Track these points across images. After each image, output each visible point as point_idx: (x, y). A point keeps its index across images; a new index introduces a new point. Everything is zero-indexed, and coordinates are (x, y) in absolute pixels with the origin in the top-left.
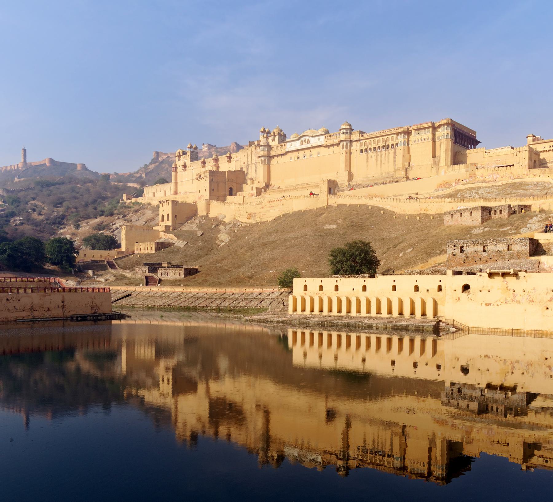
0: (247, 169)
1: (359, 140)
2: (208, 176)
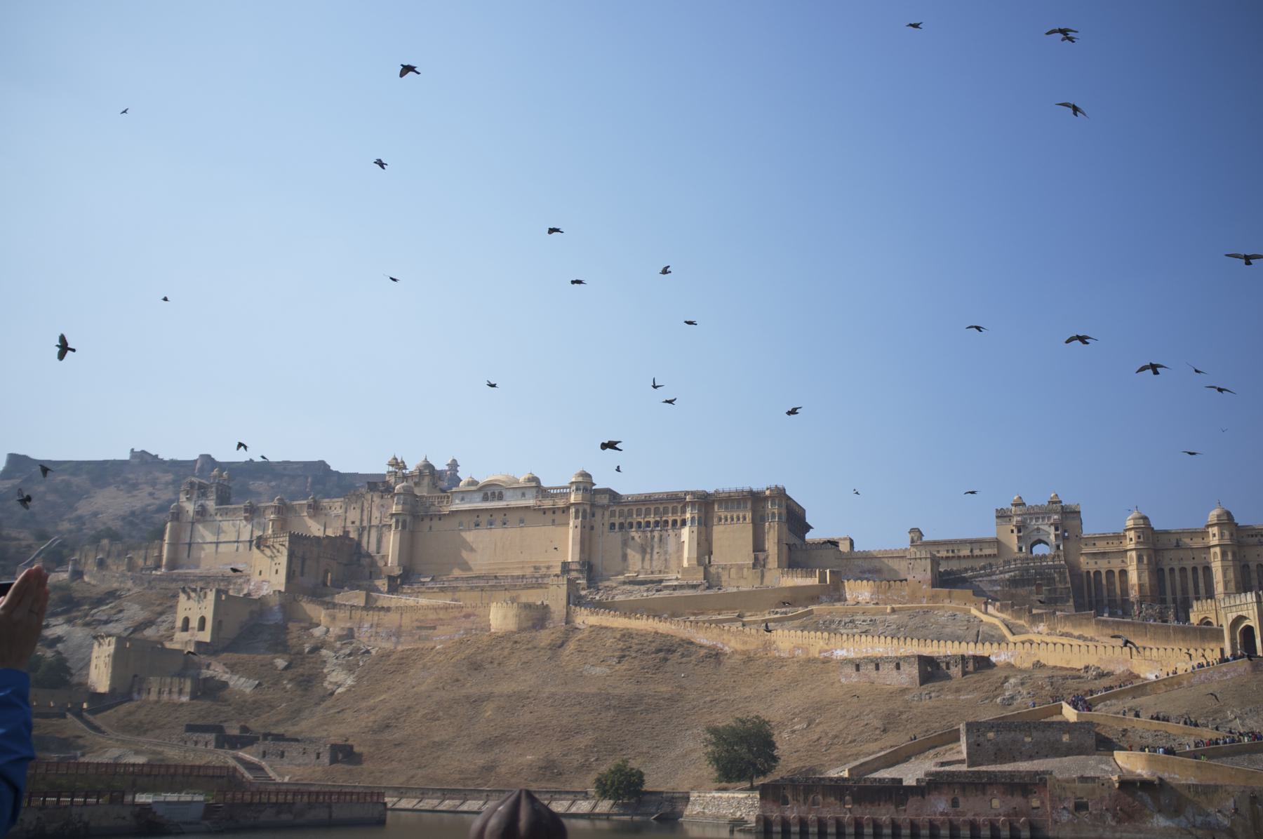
0: (360, 535)
1: (609, 506)
2: (287, 544)
